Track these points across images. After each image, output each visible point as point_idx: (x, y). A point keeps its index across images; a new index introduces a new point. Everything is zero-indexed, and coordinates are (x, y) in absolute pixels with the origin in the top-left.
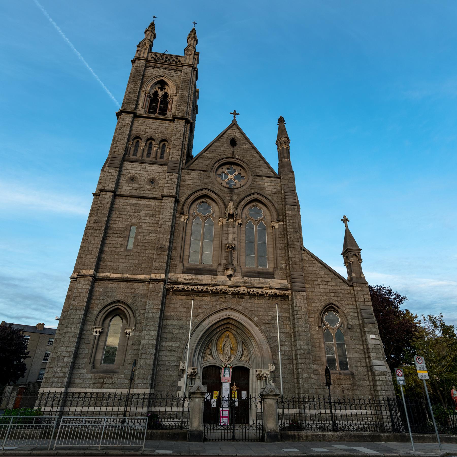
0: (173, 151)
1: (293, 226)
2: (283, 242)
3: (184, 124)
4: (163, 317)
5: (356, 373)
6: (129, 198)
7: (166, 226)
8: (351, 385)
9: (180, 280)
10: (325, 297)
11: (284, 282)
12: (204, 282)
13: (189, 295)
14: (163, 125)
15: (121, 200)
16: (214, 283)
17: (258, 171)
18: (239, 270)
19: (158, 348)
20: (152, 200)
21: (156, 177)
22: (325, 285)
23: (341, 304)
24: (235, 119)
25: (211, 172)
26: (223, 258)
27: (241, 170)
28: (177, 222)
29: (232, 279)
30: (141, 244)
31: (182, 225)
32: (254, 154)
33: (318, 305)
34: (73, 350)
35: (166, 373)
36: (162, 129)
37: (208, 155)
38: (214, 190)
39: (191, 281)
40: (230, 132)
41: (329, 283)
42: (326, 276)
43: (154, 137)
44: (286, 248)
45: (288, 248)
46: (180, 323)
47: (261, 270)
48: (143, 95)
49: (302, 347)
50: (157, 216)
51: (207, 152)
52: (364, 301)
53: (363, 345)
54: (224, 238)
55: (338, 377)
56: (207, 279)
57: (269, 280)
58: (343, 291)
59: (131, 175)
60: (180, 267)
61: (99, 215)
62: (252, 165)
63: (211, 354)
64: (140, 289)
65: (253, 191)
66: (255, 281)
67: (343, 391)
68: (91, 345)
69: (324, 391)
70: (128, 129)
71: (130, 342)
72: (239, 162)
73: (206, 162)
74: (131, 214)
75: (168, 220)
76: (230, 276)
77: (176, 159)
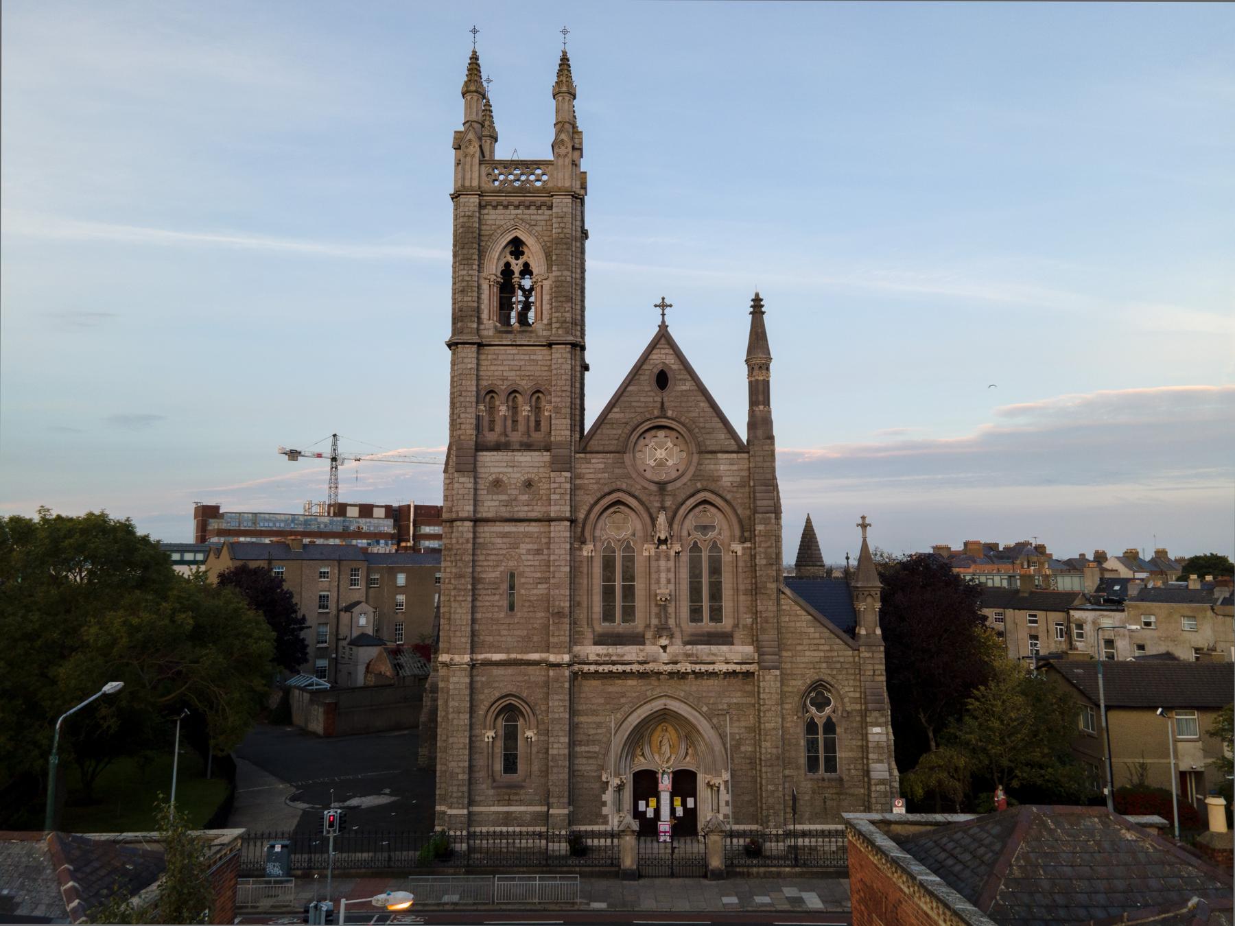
0: (557, 422)
1: (766, 553)
2: (749, 581)
3: (569, 356)
4: (573, 712)
5: (845, 778)
6: (498, 523)
7: (562, 575)
8: (836, 794)
9: (592, 658)
10: (812, 670)
11: (749, 649)
12: (625, 658)
13: (606, 678)
14: (532, 357)
15: (486, 529)
16: (641, 659)
17: (708, 442)
18: (678, 634)
19: (572, 756)
20: (533, 524)
21: (533, 476)
24: (663, 322)
25: (625, 453)
26: (653, 615)
27: (677, 438)
28: (578, 559)
29: (668, 651)
30: (527, 604)
31: (585, 564)
32: (702, 404)
33: (800, 683)
34: (466, 764)
35: (586, 785)
36: (532, 368)
37: (618, 416)
38: (633, 490)
39: (607, 658)
40: (655, 356)
41: (821, 647)
42: (817, 635)
43: (519, 389)
44: (754, 593)
45: (756, 594)
46: (597, 719)
47: (713, 630)
48: (485, 286)
49: (769, 751)
50: (545, 552)
51: (615, 410)
52: (874, 675)
53: (862, 740)
54: (653, 581)
55: (820, 785)
56: (630, 652)
57: (724, 648)
58: (842, 660)
59: (494, 476)
60: (589, 635)
61: (459, 564)
62: (697, 430)
63: (643, 755)
64: (536, 674)
65: (699, 485)
66: (702, 650)
68: (485, 754)
70: (474, 382)
71: (534, 750)
72: (674, 425)
73: (615, 432)
74: (505, 552)
75: (563, 563)
76: (664, 648)
77: (564, 438)
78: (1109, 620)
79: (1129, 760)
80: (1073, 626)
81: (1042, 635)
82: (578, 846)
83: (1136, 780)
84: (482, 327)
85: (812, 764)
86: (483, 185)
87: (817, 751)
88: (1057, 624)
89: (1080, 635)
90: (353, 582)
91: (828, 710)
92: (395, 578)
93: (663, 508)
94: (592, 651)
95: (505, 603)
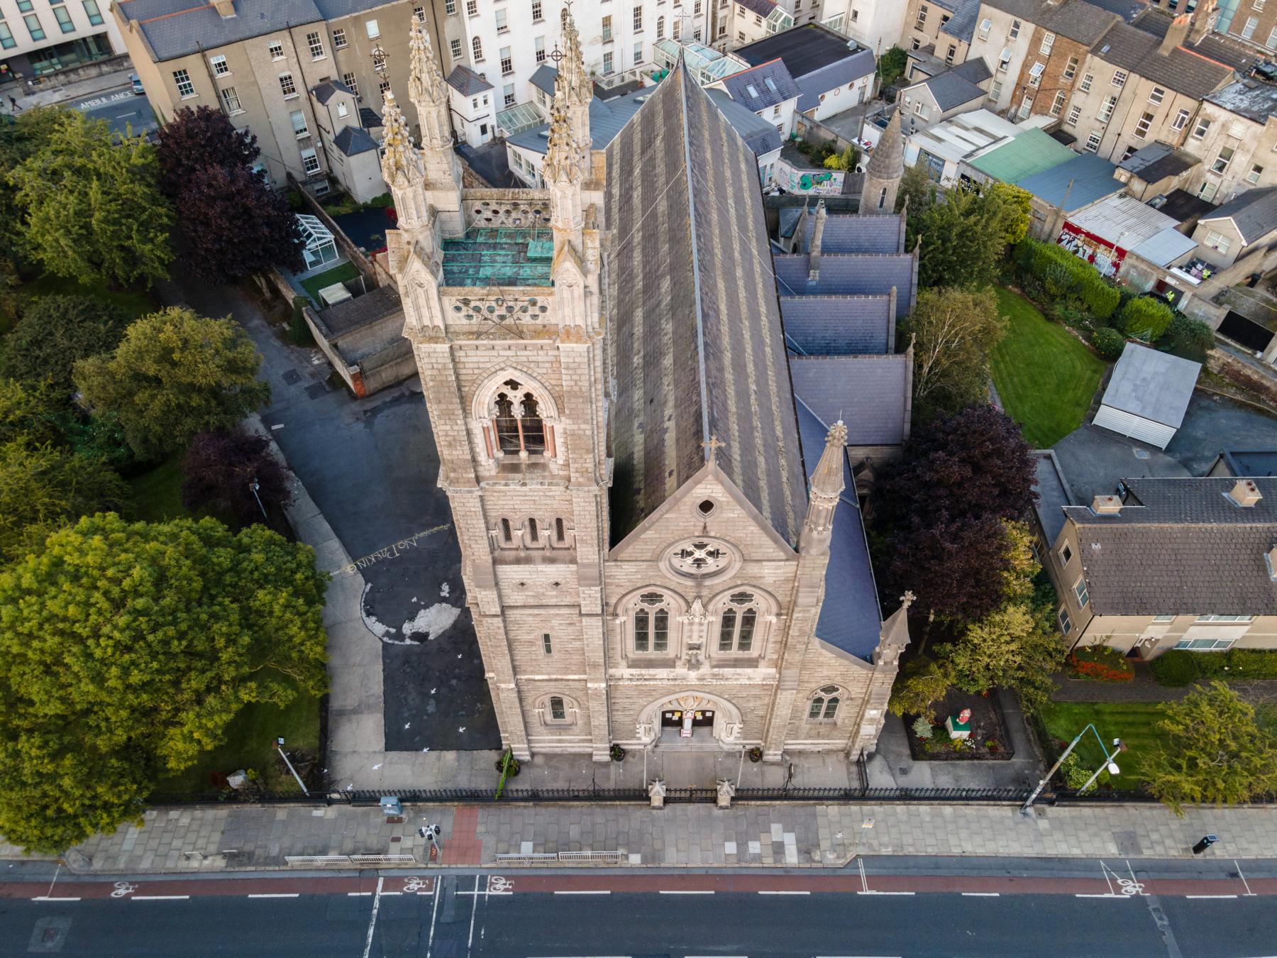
11: (773, 671)
56: (662, 673)
57: (749, 671)
65: (739, 582)
66: (728, 671)
78: (1241, 128)
79: (1098, 635)
80: (1199, 120)
81: (1158, 118)
82: (618, 753)
83: (1097, 643)
84: (480, 469)
85: (814, 714)
86: (450, 322)
88: (1182, 111)
89: (1201, 133)
90: (316, 51)
91: (835, 694)
92: (365, 30)
93: (699, 597)
94: (623, 671)
95: (543, 651)
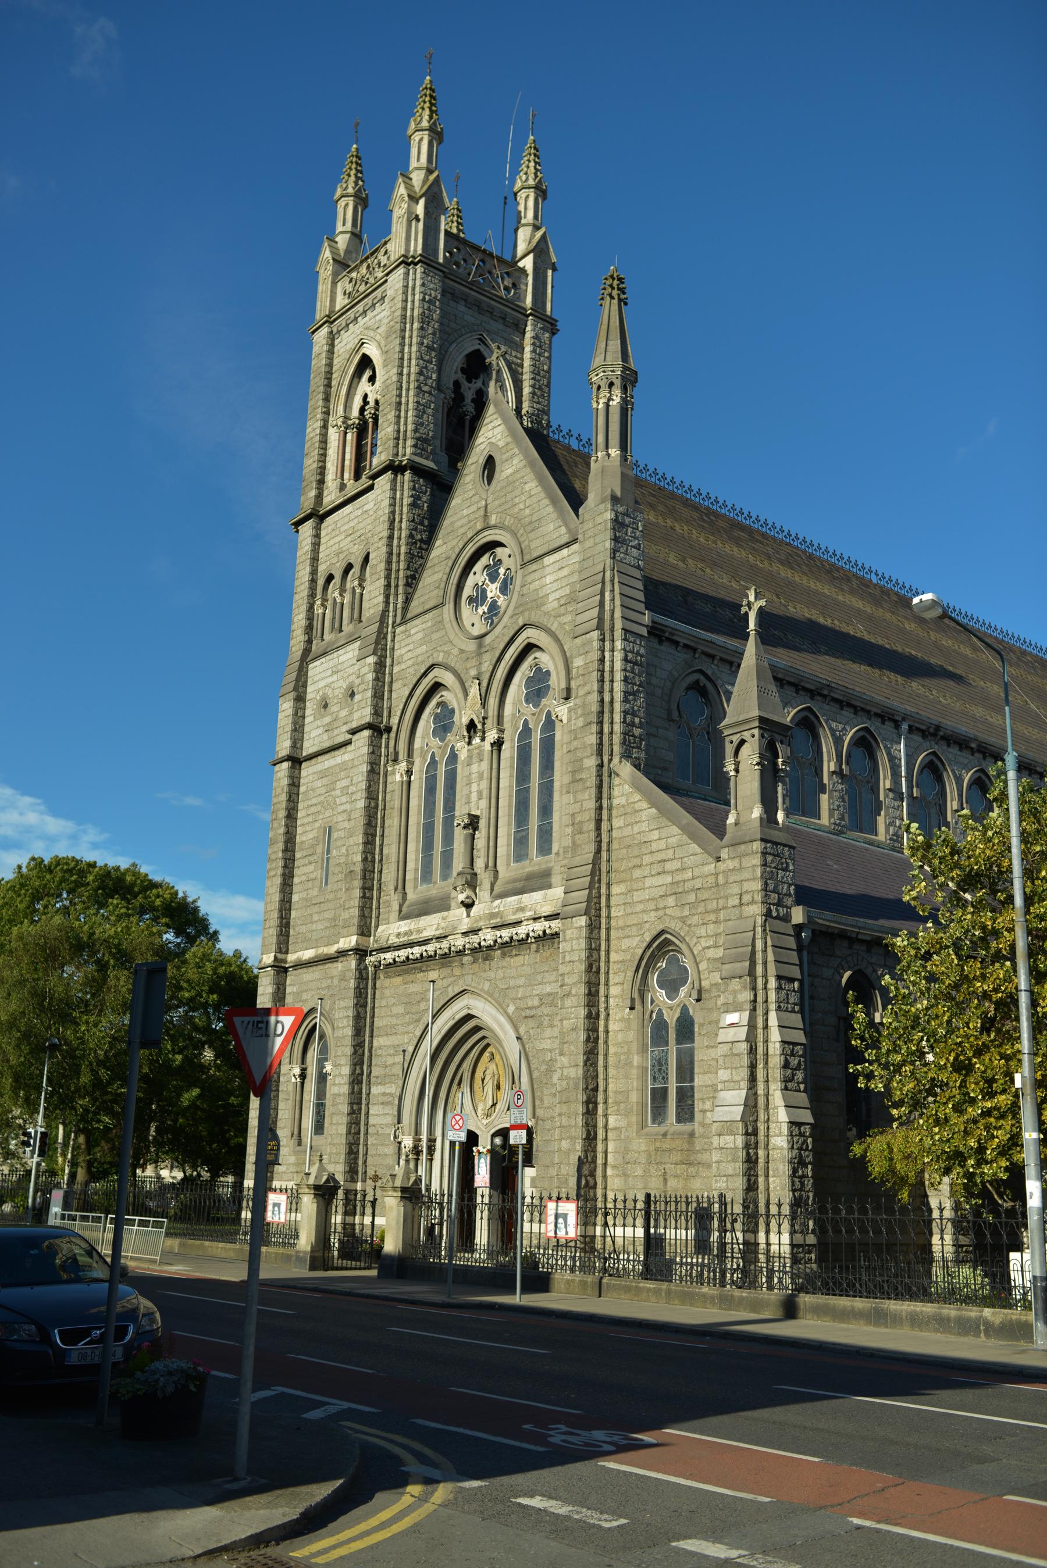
9: (394, 940)
10: (653, 914)
22: (659, 874)
23: (689, 926)
25: (442, 604)
52: (741, 905)
55: (658, 1145)
59: (321, 693)
67: (665, 1180)
69: (625, 1181)
74: (322, 798)
87: (665, 1079)
